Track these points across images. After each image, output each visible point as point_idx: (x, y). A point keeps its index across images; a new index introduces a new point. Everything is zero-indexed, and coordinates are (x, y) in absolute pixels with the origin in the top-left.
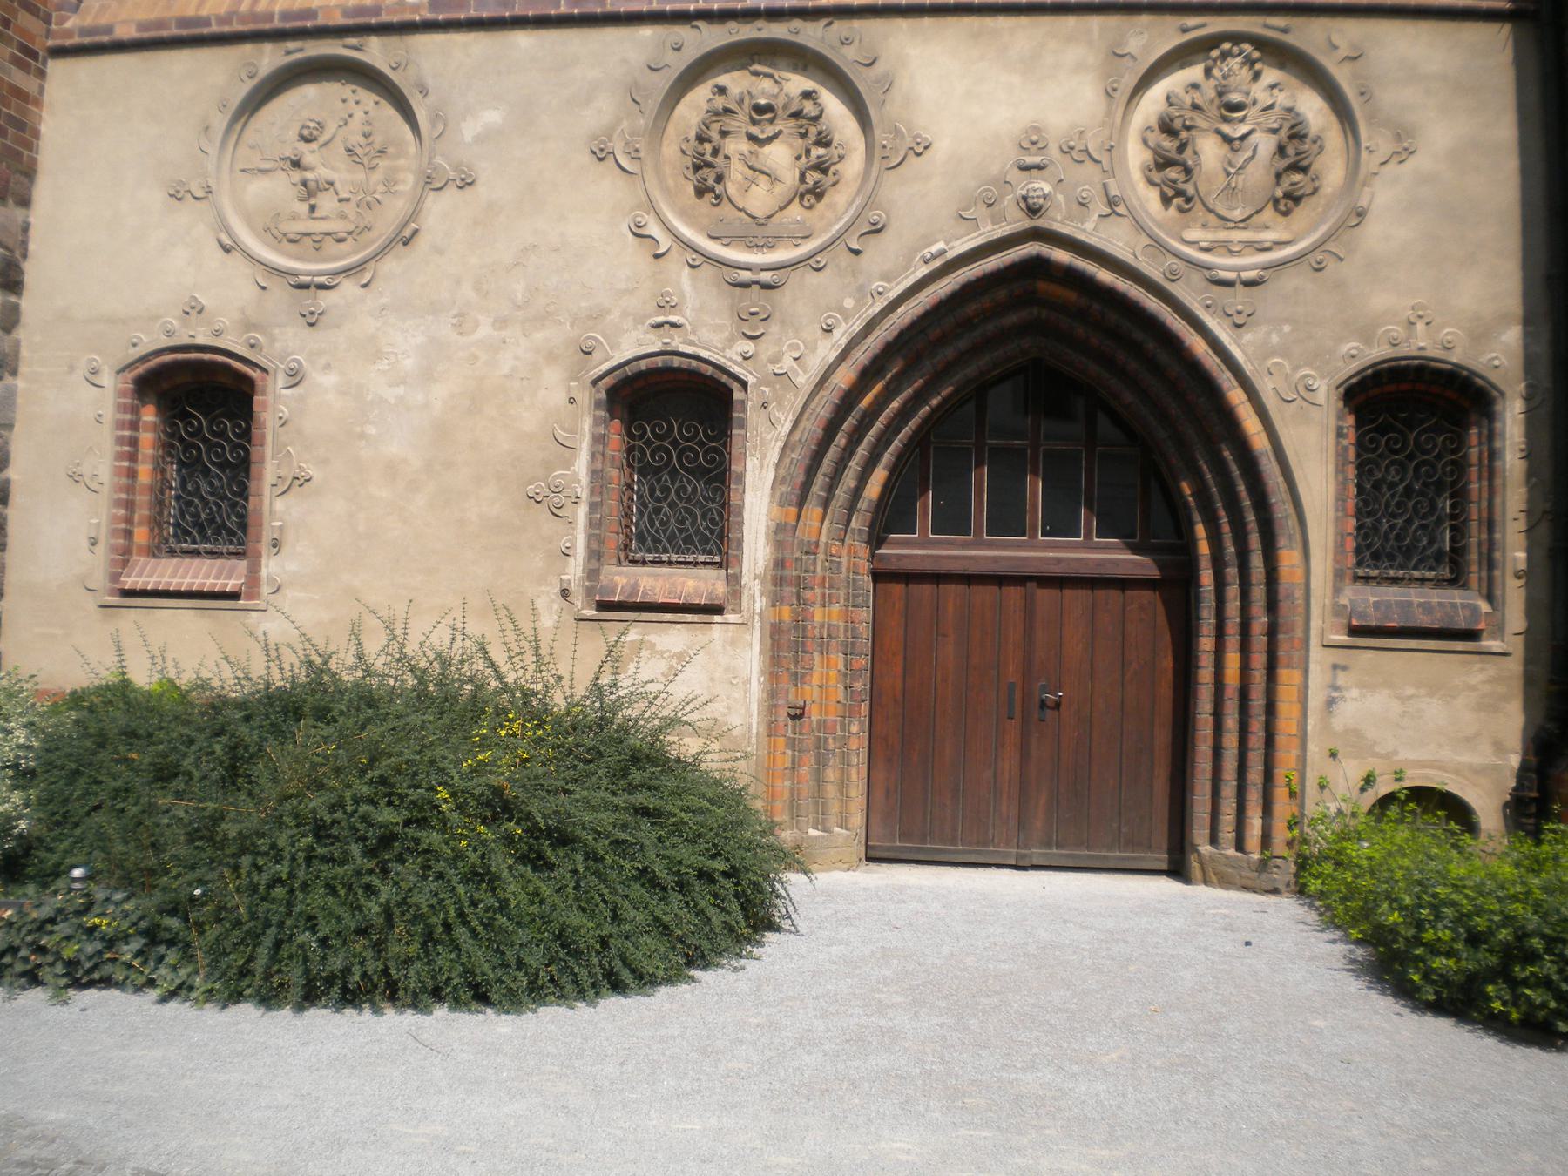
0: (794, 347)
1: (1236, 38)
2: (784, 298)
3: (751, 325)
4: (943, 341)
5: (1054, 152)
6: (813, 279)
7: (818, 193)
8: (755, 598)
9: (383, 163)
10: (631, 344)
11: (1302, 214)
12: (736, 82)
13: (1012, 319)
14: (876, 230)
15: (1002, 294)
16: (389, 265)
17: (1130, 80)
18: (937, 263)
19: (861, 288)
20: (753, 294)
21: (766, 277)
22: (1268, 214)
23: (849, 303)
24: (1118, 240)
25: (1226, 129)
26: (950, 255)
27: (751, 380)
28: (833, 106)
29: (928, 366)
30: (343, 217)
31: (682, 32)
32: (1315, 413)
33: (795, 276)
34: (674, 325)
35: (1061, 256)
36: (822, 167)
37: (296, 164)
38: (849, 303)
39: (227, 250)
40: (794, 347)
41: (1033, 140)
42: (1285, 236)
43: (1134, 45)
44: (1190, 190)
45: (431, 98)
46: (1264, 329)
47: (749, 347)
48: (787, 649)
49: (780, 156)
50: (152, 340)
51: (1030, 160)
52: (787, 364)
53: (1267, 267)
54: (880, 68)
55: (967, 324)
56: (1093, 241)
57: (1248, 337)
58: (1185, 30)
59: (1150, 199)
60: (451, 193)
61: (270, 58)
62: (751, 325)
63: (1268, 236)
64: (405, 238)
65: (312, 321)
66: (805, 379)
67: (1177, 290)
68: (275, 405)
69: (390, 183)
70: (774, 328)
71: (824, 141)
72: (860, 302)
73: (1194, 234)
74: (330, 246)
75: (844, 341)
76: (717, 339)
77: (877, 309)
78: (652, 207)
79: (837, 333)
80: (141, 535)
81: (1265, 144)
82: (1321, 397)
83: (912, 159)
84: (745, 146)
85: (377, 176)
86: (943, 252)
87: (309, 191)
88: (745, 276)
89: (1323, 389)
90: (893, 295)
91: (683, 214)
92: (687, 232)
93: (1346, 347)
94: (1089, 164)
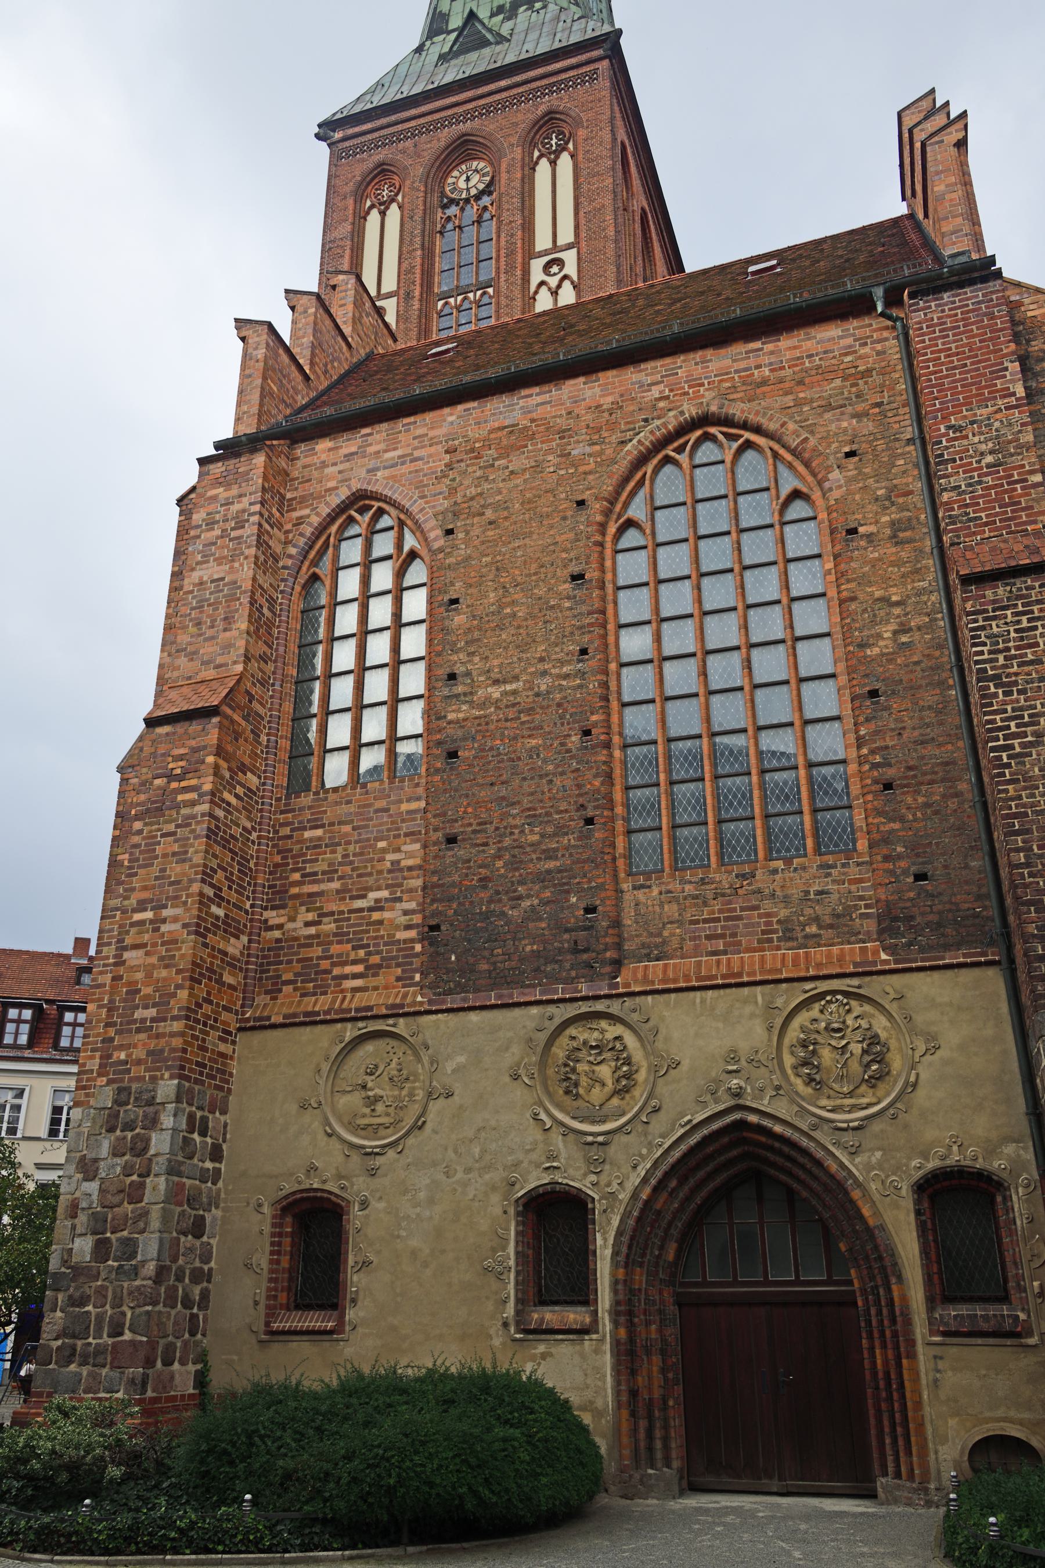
0: (618, 1177)
1: (834, 992)
2: (612, 1150)
3: (596, 1165)
4: (698, 1167)
5: (743, 1063)
6: (624, 1139)
7: (627, 1090)
8: (606, 1324)
9: (408, 1085)
10: (535, 1180)
11: (882, 1087)
12: (581, 1033)
13: (735, 1153)
14: (656, 1110)
15: (726, 1140)
16: (411, 1141)
17: (778, 1022)
18: (688, 1127)
19: (650, 1143)
20: (596, 1150)
21: (600, 1139)
22: (864, 1088)
23: (644, 1151)
24: (782, 1109)
25: (834, 1043)
26: (695, 1122)
27: (596, 1197)
28: (630, 1040)
29: (692, 1182)
30: (388, 1115)
31: (551, 1009)
32: (903, 1203)
33: (616, 1137)
34: (555, 1168)
35: (753, 1118)
36: (628, 1076)
37: (364, 1087)
38: (644, 1151)
39: (330, 1135)
40: (618, 1177)
41: (733, 1056)
42: (874, 1100)
43: (779, 1002)
44: (818, 1077)
45: (430, 1051)
46: (867, 1154)
47: (593, 1178)
48: (628, 1357)
49: (605, 1071)
50: (289, 1187)
51: (730, 1068)
52: (615, 1187)
53: (862, 1119)
54: (651, 1024)
55: (710, 1157)
56: (768, 1110)
57: (858, 1160)
58: (806, 992)
59: (799, 1083)
60: (441, 1101)
61: (350, 1032)
62: (596, 1165)
63: (864, 1101)
64: (418, 1126)
65: (373, 1172)
66: (624, 1196)
67: (817, 1134)
69: (411, 1095)
70: (607, 1167)
71: (628, 1061)
72: (650, 1152)
73: (824, 1102)
74: (382, 1132)
75: (643, 1173)
76: (578, 1174)
77: (659, 1153)
78: (541, 1104)
79: (639, 1168)
80: (283, 1298)
81: (857, 1048)
82: (904, 1192)
83: (672, 1071)
84: (586, 1068)
85: (404, 1092)
86: (690, 1121)
87: (372, 1102)
88: (590, 1139)
89: (905, 1188)
90: (666, 1146)
91: (559, 1106)
92: (560, 1116)
93: (915, 1163)
94: (763, 1068)
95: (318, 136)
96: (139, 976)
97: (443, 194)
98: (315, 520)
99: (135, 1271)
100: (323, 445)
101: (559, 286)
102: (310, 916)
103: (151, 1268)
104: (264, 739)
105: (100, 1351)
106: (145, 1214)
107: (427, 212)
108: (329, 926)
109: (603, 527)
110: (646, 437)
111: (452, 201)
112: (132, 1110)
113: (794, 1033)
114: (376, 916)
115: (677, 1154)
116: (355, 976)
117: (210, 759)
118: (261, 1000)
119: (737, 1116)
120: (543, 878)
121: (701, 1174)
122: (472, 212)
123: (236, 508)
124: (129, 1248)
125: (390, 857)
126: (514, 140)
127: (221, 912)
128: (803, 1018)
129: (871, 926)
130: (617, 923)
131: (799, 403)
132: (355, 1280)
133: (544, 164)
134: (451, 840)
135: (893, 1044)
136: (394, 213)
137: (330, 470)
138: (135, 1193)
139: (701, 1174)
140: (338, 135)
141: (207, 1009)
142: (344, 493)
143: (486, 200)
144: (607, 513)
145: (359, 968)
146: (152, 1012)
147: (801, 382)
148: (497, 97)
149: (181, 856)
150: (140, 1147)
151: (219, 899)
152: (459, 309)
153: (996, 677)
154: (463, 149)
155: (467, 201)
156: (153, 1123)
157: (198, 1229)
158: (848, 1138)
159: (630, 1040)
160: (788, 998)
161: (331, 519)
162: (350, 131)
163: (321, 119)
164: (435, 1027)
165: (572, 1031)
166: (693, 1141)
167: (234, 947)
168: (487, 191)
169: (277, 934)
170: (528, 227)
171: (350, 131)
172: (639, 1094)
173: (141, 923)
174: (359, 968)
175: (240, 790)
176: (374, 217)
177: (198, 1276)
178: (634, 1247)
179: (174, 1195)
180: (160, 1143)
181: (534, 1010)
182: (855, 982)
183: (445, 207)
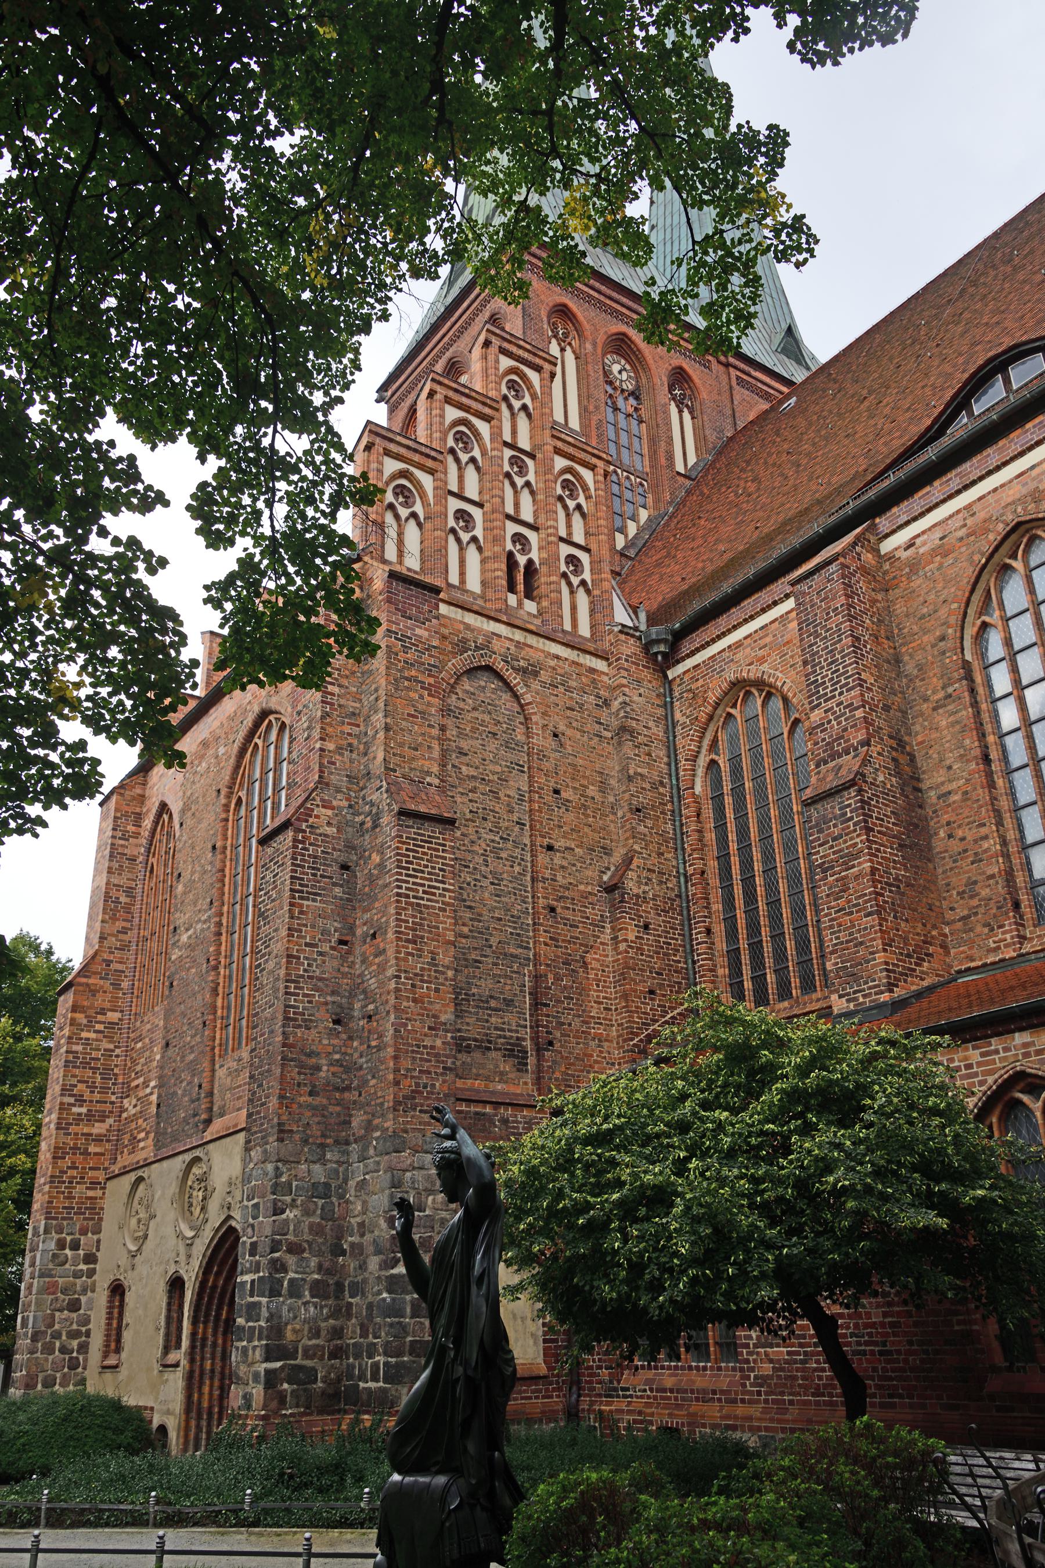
8: (184, 1362)
49: (200, 1194)
95: (378, 401)
127: (84, 1110)
151: (80, 1101)
157: (74, 1306)
162: (394, 387)
167: (98, 1129)
171: (394, 387)
177: (73, 1335)
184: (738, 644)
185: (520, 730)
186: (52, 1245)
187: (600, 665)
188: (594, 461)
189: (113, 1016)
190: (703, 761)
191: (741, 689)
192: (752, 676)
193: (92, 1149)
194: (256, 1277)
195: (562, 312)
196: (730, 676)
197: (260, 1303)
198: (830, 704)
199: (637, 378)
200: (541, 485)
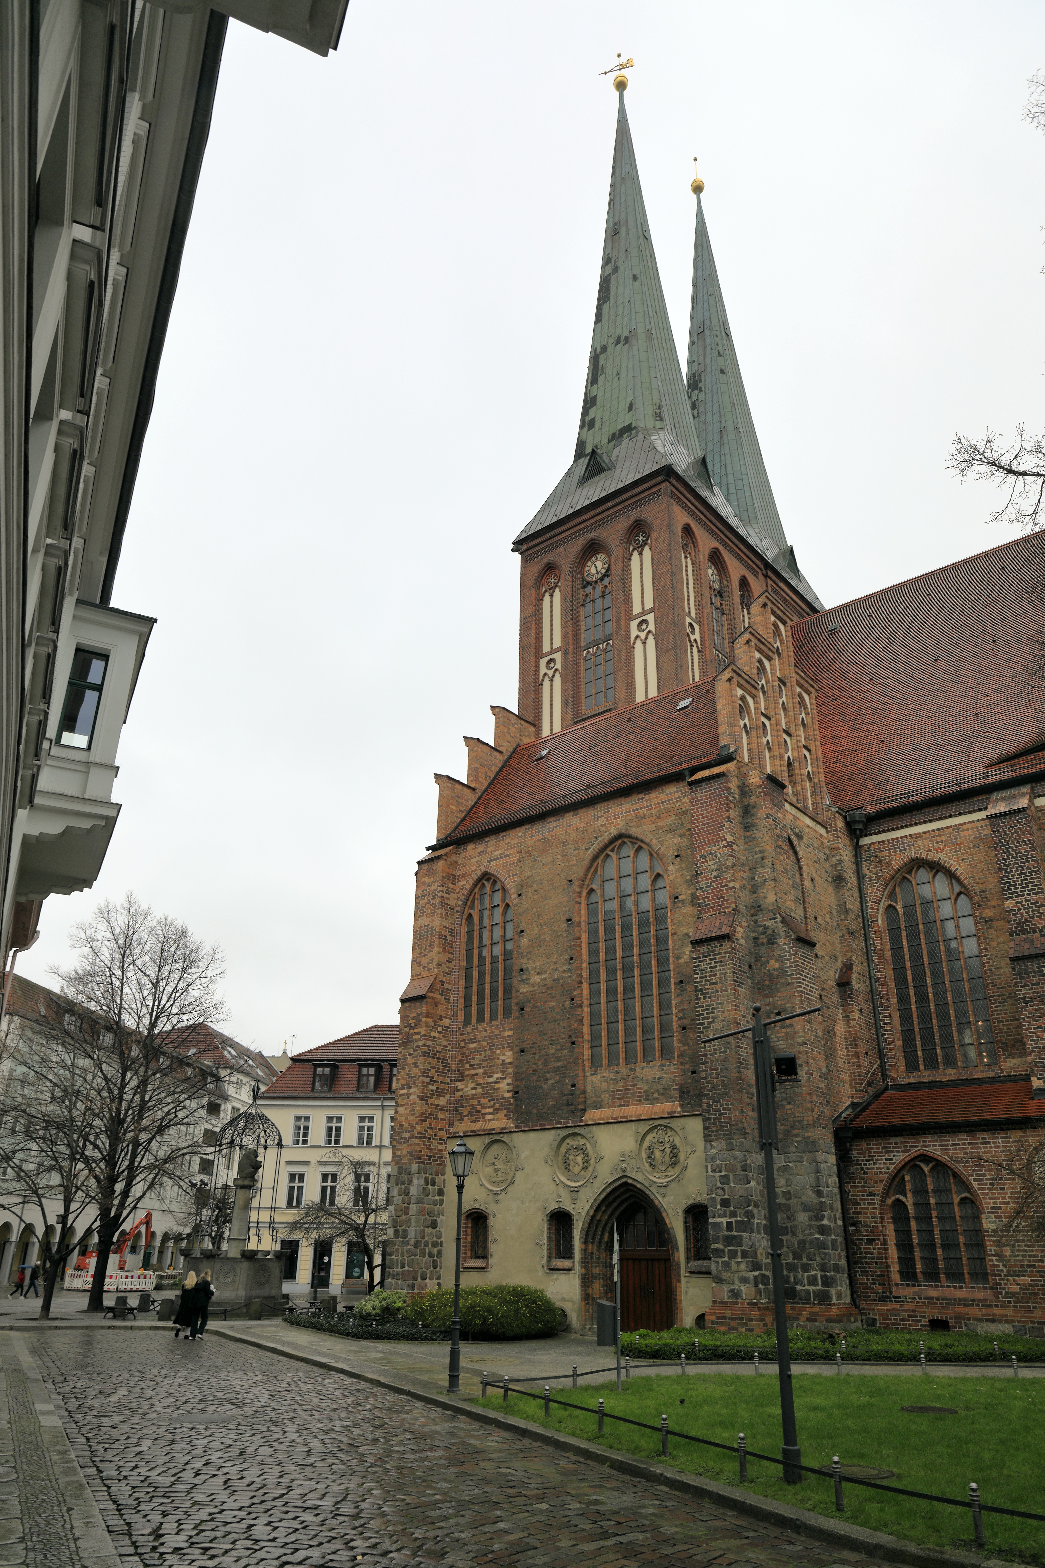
3: (574, 1200)
8: (577, 1267)
10: (553, 1206)
16: (510, 1188)
24: (639, 1177)
31: (559, 1131)
35: (630, 1181)
48: (586, 1281)
49: (579, 1159)
62: (574, 1200)
65: (497, 1202)
66: (584, 1214)
68: (491, 1221)
71: (587, 1156)
81: (668, 1150)
87: (496, 1171)
95: (513, 550)
96: (403, 1118)
97: (583, 579)
98: (468, 887)
99: (407, 1243)
100: (471, 846)
101: (646, 638)
102: (473, 1085)
103: (412, 1241)
104: (451, 1000)
105: (398, 1274)
106: (410, 1220)
107: (574, 593)
108: (480, 1090)
109: (580, 893)
110: (596, 847)
111: (589, 583)
112: (405, 1177)
113: (646, 1144)
114: (497, 1085)
115: (603, 1196)
116: (490, 1114)
117: (424, 1019)
118: (457, 1123)
119: (624, 1180)
120: (556, 1070)
121: (615, 1204)
122: (599, 588)
123: (432, 888)
124: (405, 1234)
125: (502, 1058)
126: (617, 542)
127: (434, 1088)
128: (650, 1137)
129: (676, 1094)
130: (584, 1092)
131: (658, 829)
132: (492, 1248)
133: (636, 553)
134: (522, 1051)
135: (681, 1149)
136: (557, 594)
137: (474, 860)
138: (406, 1211)
139: (615, 1204)
140: (524, 547)
141: (430, 1131)
142: (479, 873)
143: (606, 581)
144: (581, 887)
145: (491, 1110)
146: (408, 1135)
147: (658, 817)
148: (607, 513)
149: (415, 1065)
150: (407, 1193)
151: (433, 1081)
152: (595, 655)
153: (701, 990)
154: (593, 548)
155: (596, 582)
156: (410, 1182)
157: (434, 1225)
158: (662, 1190)
159: (588, 1145)
160: (644, 1127)
161: (475, 886)
163: (513, 539)
164: (518, 1139)
165: (568, 1141)
166: (608, 1190)
167: (442, 1101)
168: (606, 575)
169: (461, 1093)
170: (628, 600)
172: (591, 1169)
173: (402, 1095)
174: (491, 1110)
175: (440, 1029)
176: (547, 598)
177: (435, 1244)
178: (588, 1236)
179: (421, 1212)
180: (413, 1190)
181: (553, 1132)
182: (667, 1121)
183: (584, 587)
184: (918, 836)
185: (798, 876)
186: (422, 1182)
187: (822, 831)
188: (811, 689)
189: (447, 1022)
190: (883, 905)
191: (918, 864)
192: (930, 858)
193: (440, 1116)
194: (733, 1220)
195: (687, 529)
196: (912, 854)
197: (741, 1237)
198: (1020, 899)
199: (721, 581)
200: (791, 705)
